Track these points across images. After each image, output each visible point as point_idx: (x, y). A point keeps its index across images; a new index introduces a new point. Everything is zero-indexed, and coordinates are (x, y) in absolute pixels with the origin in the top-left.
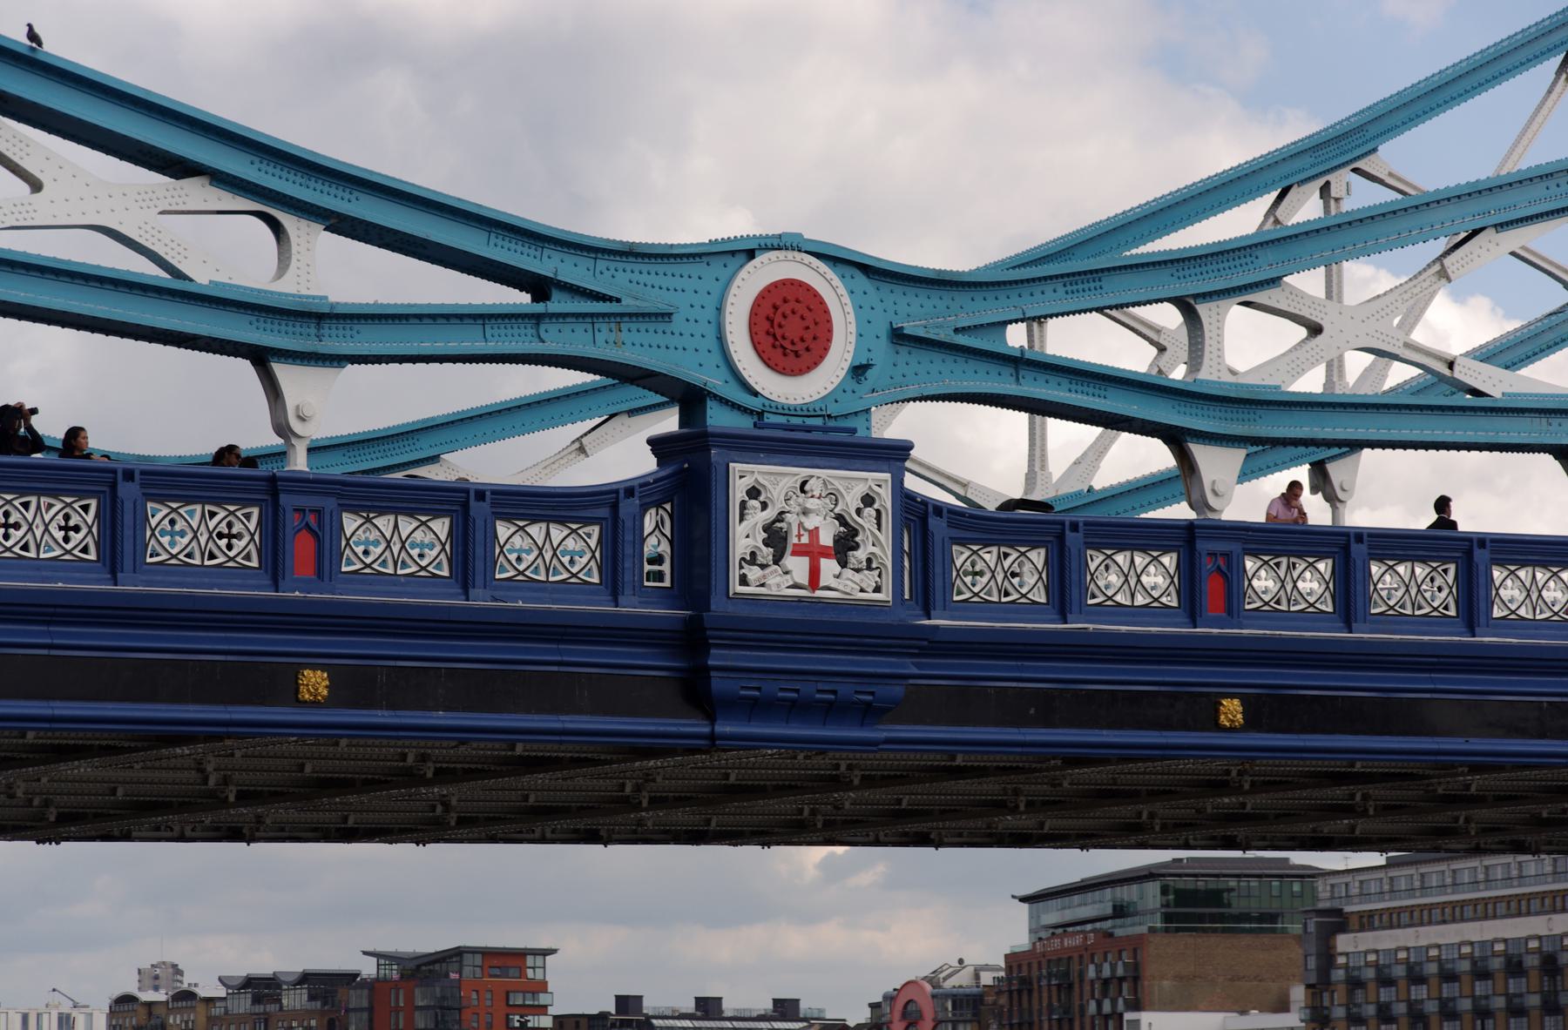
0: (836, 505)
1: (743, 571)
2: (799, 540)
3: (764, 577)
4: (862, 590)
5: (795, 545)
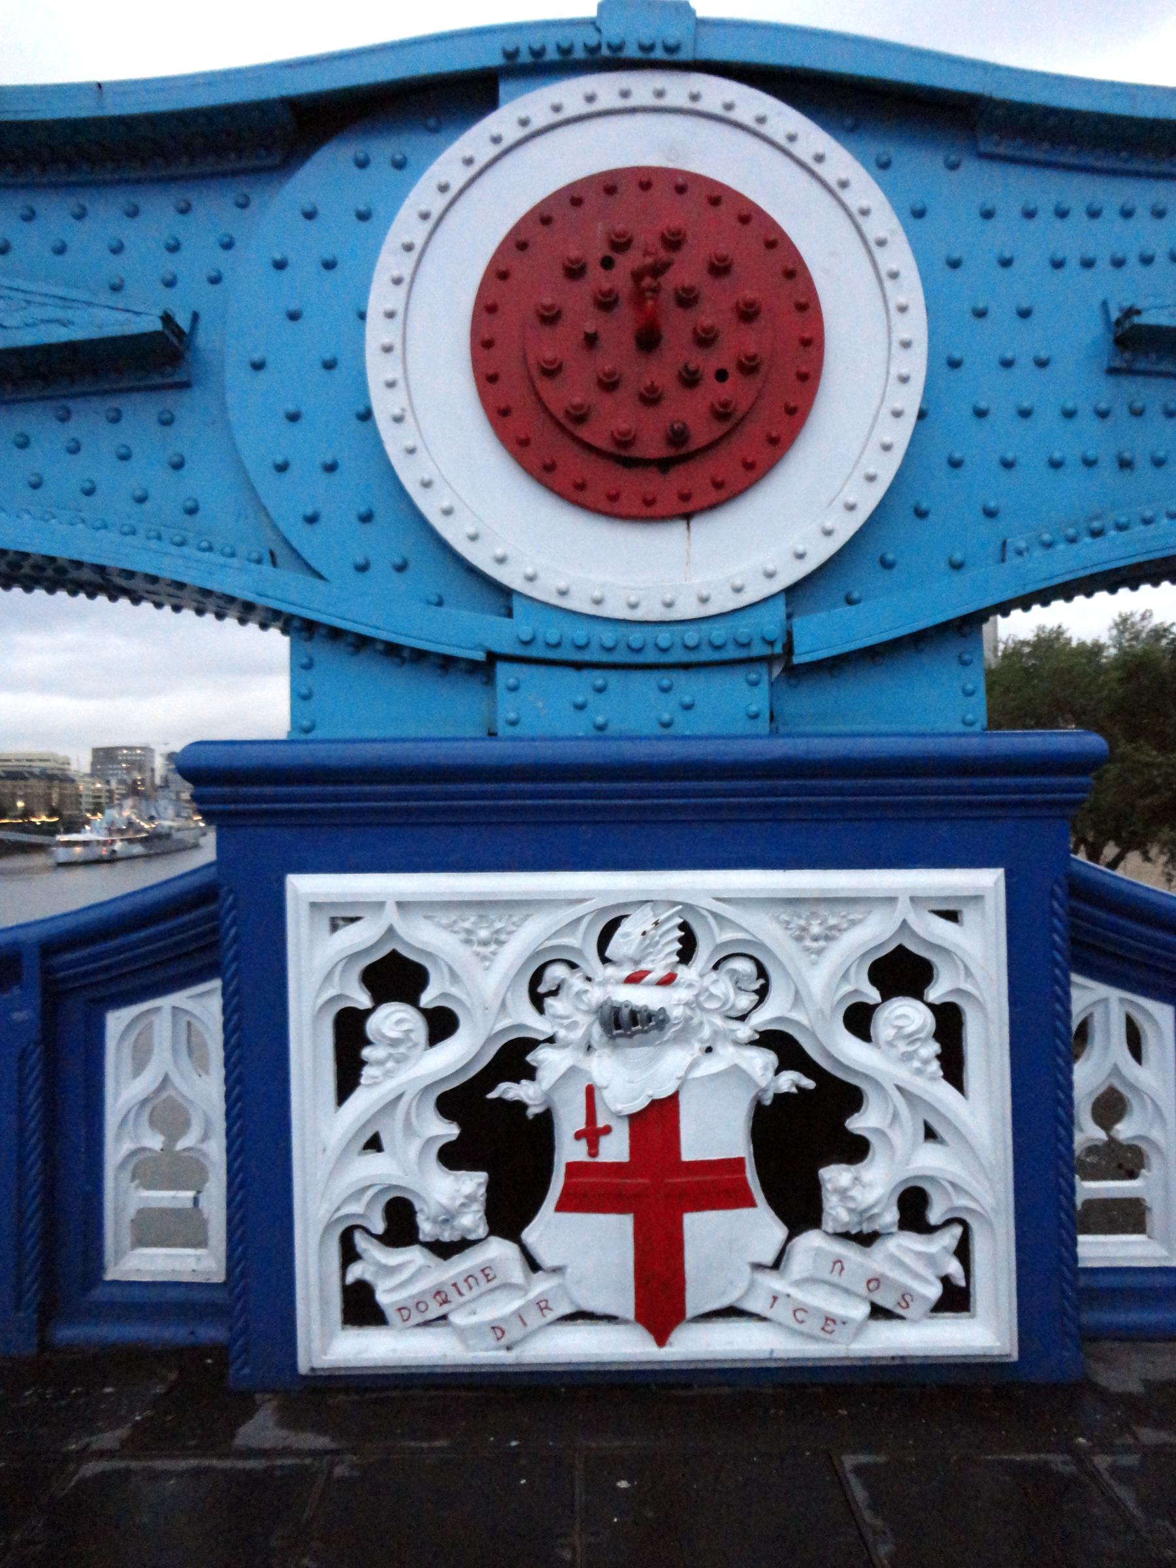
0: (763, 993)
1: (356, 1272)
2: (593, 1149)
3: (439, 1294)
4: (878, 1312)
5: (573, 1169)
